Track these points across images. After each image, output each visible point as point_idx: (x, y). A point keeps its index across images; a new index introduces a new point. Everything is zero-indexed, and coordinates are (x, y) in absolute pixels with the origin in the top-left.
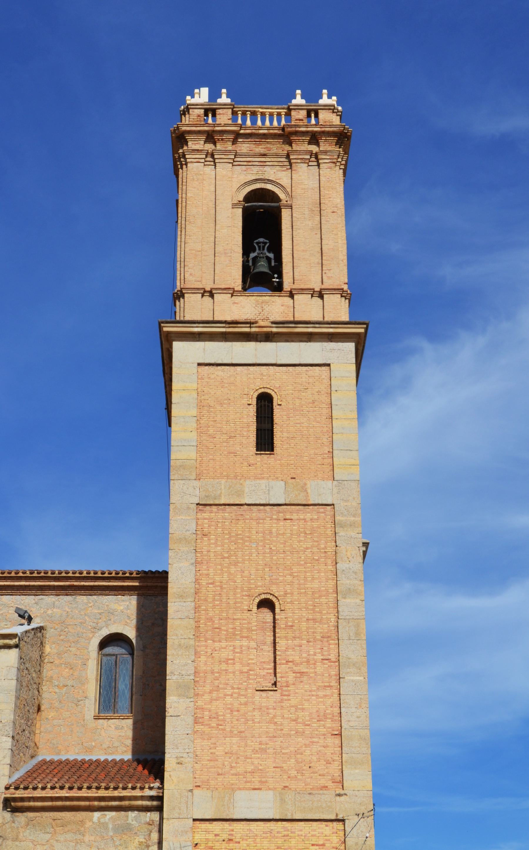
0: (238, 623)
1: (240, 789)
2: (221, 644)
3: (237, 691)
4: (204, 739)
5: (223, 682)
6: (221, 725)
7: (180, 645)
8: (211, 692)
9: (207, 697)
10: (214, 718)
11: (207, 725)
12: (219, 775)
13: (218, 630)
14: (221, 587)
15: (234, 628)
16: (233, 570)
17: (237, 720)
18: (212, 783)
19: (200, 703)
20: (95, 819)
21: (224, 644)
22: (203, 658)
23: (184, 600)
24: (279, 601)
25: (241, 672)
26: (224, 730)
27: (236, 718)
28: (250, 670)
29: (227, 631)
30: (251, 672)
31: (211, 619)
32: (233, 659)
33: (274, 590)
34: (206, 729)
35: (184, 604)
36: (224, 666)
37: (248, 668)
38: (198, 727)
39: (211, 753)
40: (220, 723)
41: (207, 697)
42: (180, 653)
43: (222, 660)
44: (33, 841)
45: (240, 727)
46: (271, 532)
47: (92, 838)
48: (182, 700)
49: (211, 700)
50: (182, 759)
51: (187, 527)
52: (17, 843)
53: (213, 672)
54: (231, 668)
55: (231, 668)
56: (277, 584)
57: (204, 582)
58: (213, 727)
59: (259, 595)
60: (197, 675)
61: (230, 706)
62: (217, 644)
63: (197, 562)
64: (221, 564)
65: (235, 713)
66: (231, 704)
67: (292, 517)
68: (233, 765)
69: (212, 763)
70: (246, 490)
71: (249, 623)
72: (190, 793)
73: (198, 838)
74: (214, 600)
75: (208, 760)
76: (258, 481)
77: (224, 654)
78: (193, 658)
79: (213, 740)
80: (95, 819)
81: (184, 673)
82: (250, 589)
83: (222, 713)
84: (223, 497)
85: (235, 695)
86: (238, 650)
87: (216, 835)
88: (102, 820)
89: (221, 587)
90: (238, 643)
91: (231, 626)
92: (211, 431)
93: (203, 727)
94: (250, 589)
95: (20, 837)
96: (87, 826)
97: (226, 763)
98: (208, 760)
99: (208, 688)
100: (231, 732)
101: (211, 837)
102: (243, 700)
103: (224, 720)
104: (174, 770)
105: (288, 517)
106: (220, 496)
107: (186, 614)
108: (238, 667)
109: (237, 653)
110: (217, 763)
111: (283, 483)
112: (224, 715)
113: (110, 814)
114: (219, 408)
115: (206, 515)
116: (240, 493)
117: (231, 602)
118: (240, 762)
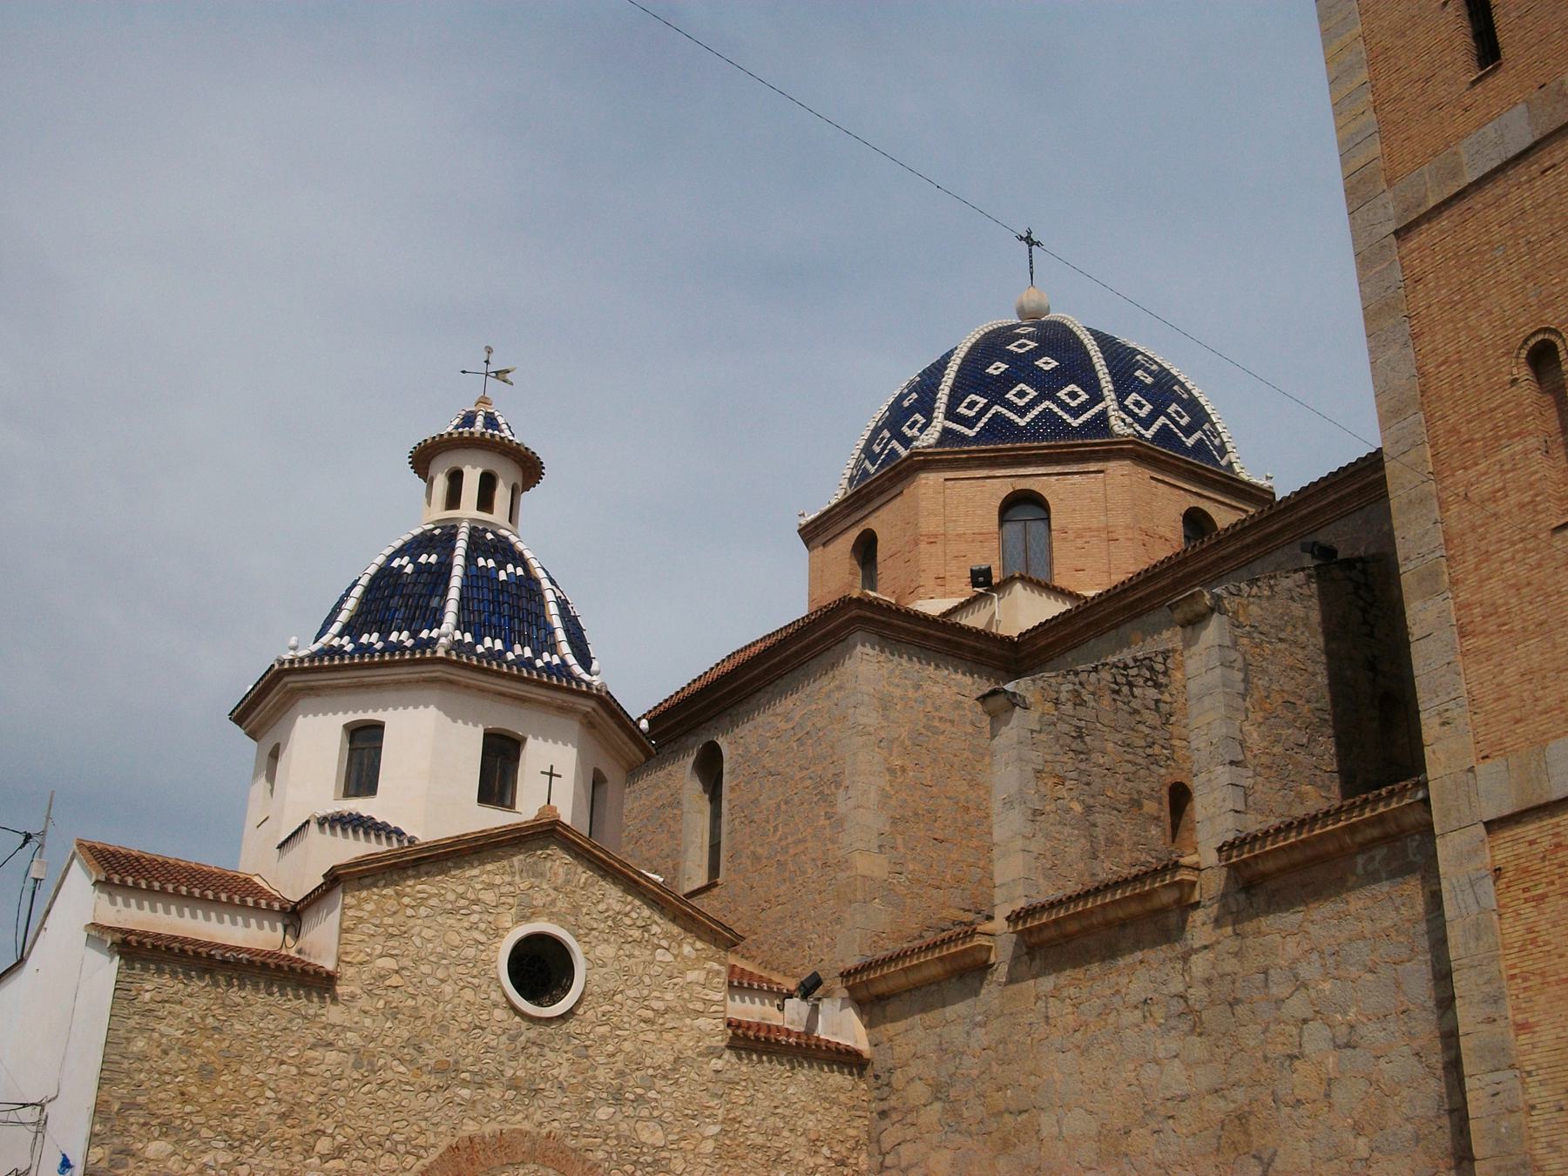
0: (1499, 415)
1: (1558, 737)
2: (1478, 467)
3: (1521, 545)
4: (1482, 663)
5: (1494, 539)
6: (1505, 624)
7: (1410, 501)
8: (1476, 569)
9: (1472, 580)
10: (1491, 615)
11: (1481, 634)
12: (1517, 722)
13: (1469, 444)
14: (1460, 361)
15: (1496, 427)
16: (1473, 315)
17: (1531, 603)
18: (1509, 741)
19: (1463, 596)
20: (1360, 870)
21: (1482, 467)
22: (1454, 509)
23: (1404, 416)
24: (1561, 336)
25: (1522, 506)
26: (1510, 631)
27: (1528, 599)
28: (1537, 495)
29: (1483, 439)
30: (1538, 499)
31: (1454, 431)
32: (1504, 488)
33: (1550, 318)
34: (1480, 642)
35: (1405, 424)
36: (1491, 507)
37: (1532, 493)
38: (1470, 643)
39: (1498, 685)
40: (1502, 620)
41: (1472, 580)
42: (1412, 516)
43: (1486, 497)
44: (1279, 931)
45: (1537, 615)
46: (1524, 212)
47: (1361, 904)
48: (1430, 603)
49: (1481, 581)
50: (1448, 714)
51: (1386, 284)
52: (1260, 940)
53: (1473, 530)
54: (1502, 508)
55: (1502, 508)
56: (1552, 304)
57: (1430, 368)
58: (1492, 634)
59: (1525, 342)
60: (1450, 546)
61: (1513, 581)
62: (1472, 472)
63: (1415, 337)
64: (1450, 320)
65: (1525, 590)
66: (1515, 575)
67: (1555, 161)
68: (1539, 694)
69: (1502, 704)
70: (1465, 159)
71: (1519, 405)
72: (1470, 775)
73: (1501, 857)
74: (1453, 390)
75: (1496, 700)
76: (1481, 131)
77: (1486, 487)
78: (1437, 514)
79: (1496, 659)
80: (1360, 870)
81: (1424, 550)
82: (1507, 339)
83: (1502, 601)
84: (1430, 194)
85: (1519, 556)
86: (1506, 467)
87: (1531, 843)
88: (1370, 868)
89: (1460, 361)
90: (1506, 453)
91: (1489, 426)
92: (1396, 90)
93: (1475, 640)
94: (1507, 339)
95: (1263, 929)
96: (1350, 884)
97: (1525, 695)
98: (1496, 700)
99: (1471, 560)
100: (1524, 629)
101: (1522, 848)
102: (1533, 559)
103: (1508, 612)
104: (1438, 739)
105: (1547, 165)
106: (1426, 196)
107: (1410, 441)
108: (1513, 498)
109: (1508, 472)
110: (1508, 700)
111: (1522, 107)
112: (1506, 604)
113: (1381, 853)
114: (1401, 42)
115: (1412, 244)
116: (1455, 173)
117: (1481, 380)
118: (1550, 684)
